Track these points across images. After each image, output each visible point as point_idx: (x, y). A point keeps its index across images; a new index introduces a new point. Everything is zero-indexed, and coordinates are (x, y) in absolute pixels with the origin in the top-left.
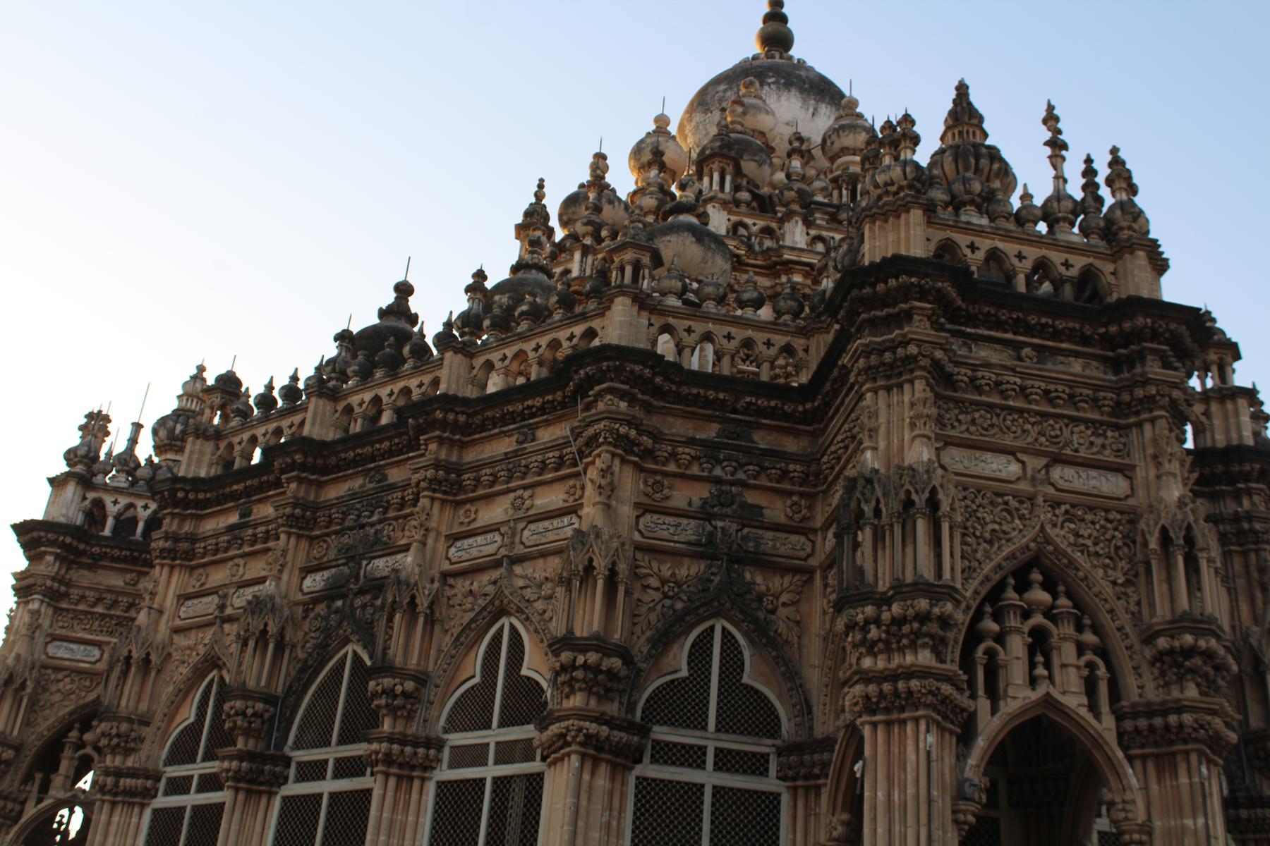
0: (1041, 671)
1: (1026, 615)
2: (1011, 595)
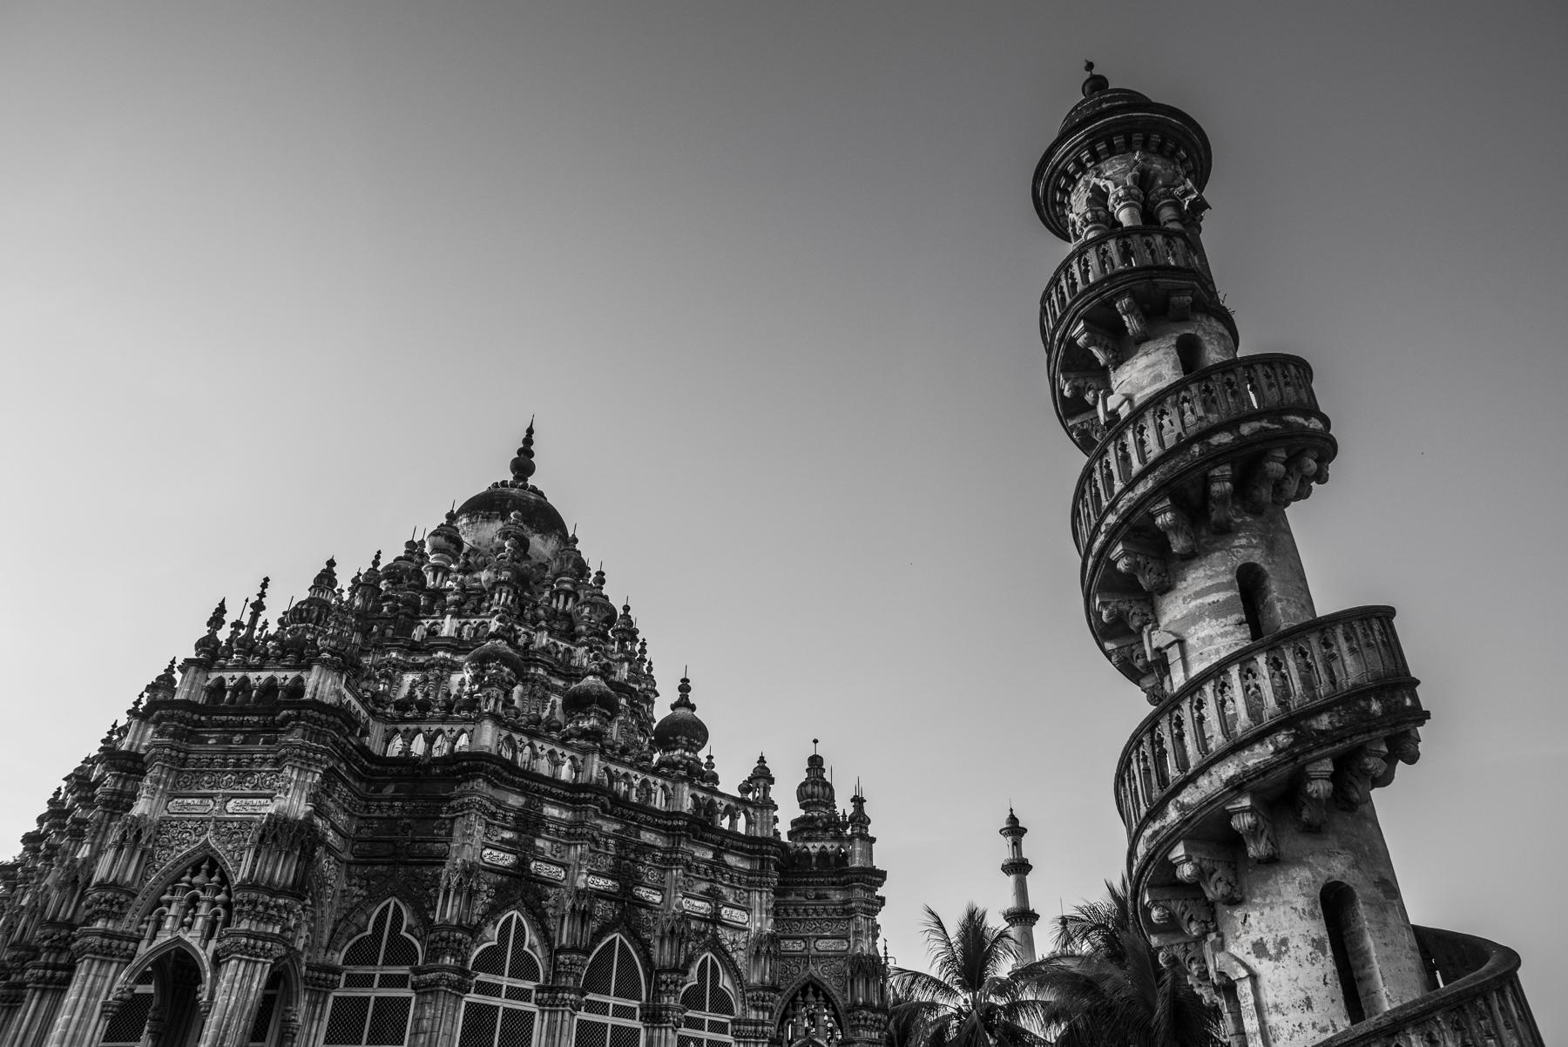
0: (188, 919)
1: (188, 889)
2: (187, 878)
